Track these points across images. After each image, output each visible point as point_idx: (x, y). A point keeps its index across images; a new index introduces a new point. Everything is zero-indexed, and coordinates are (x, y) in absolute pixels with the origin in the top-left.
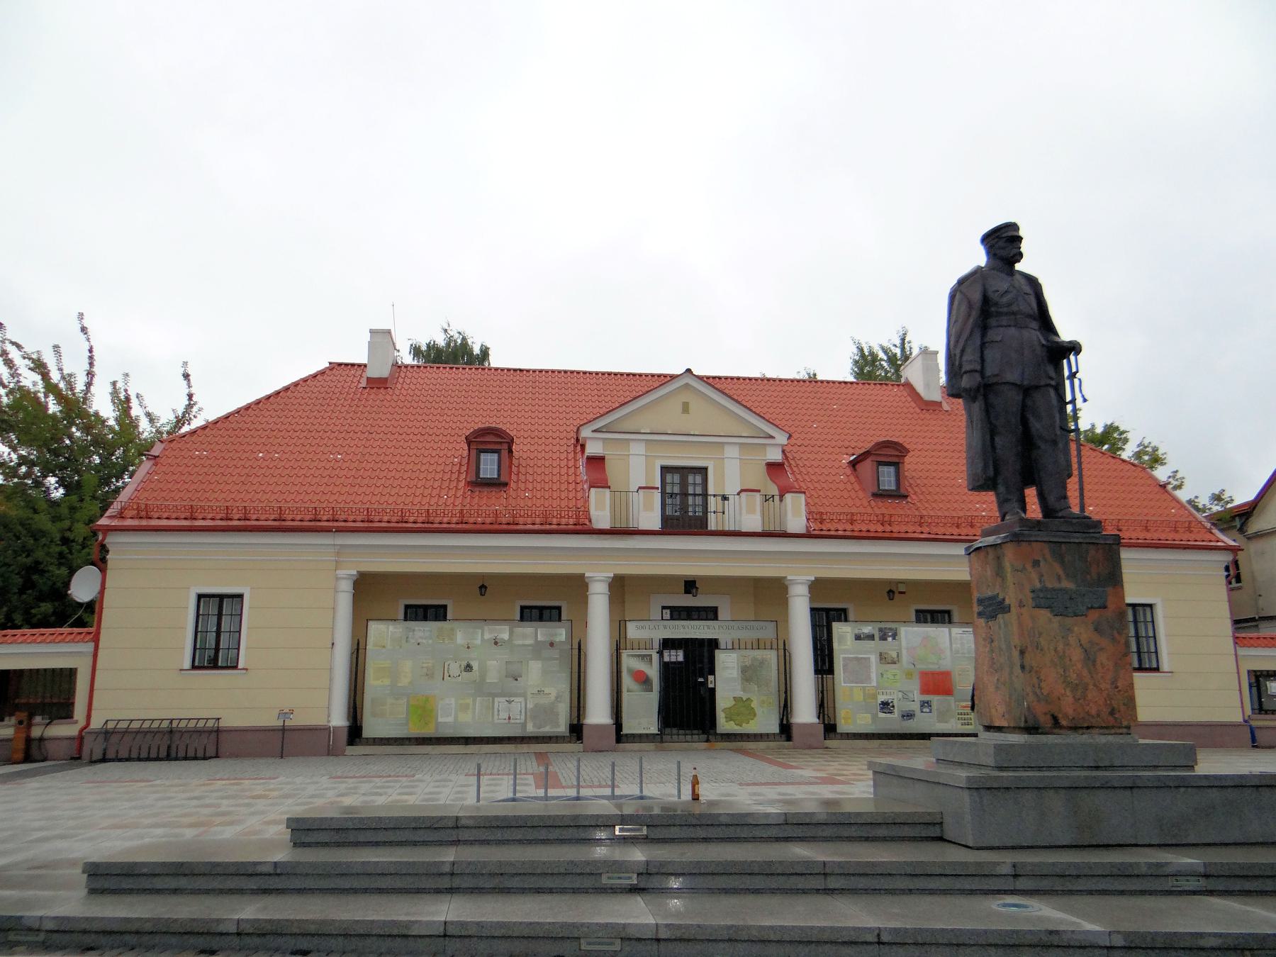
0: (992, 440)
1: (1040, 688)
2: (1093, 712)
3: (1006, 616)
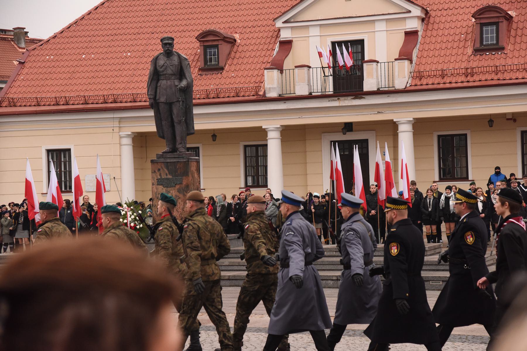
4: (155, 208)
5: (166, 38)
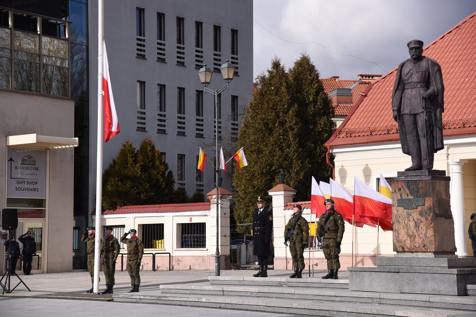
1: (398, 237)
2: (417, 246)
4: (395, 233)
5: (412, 42)
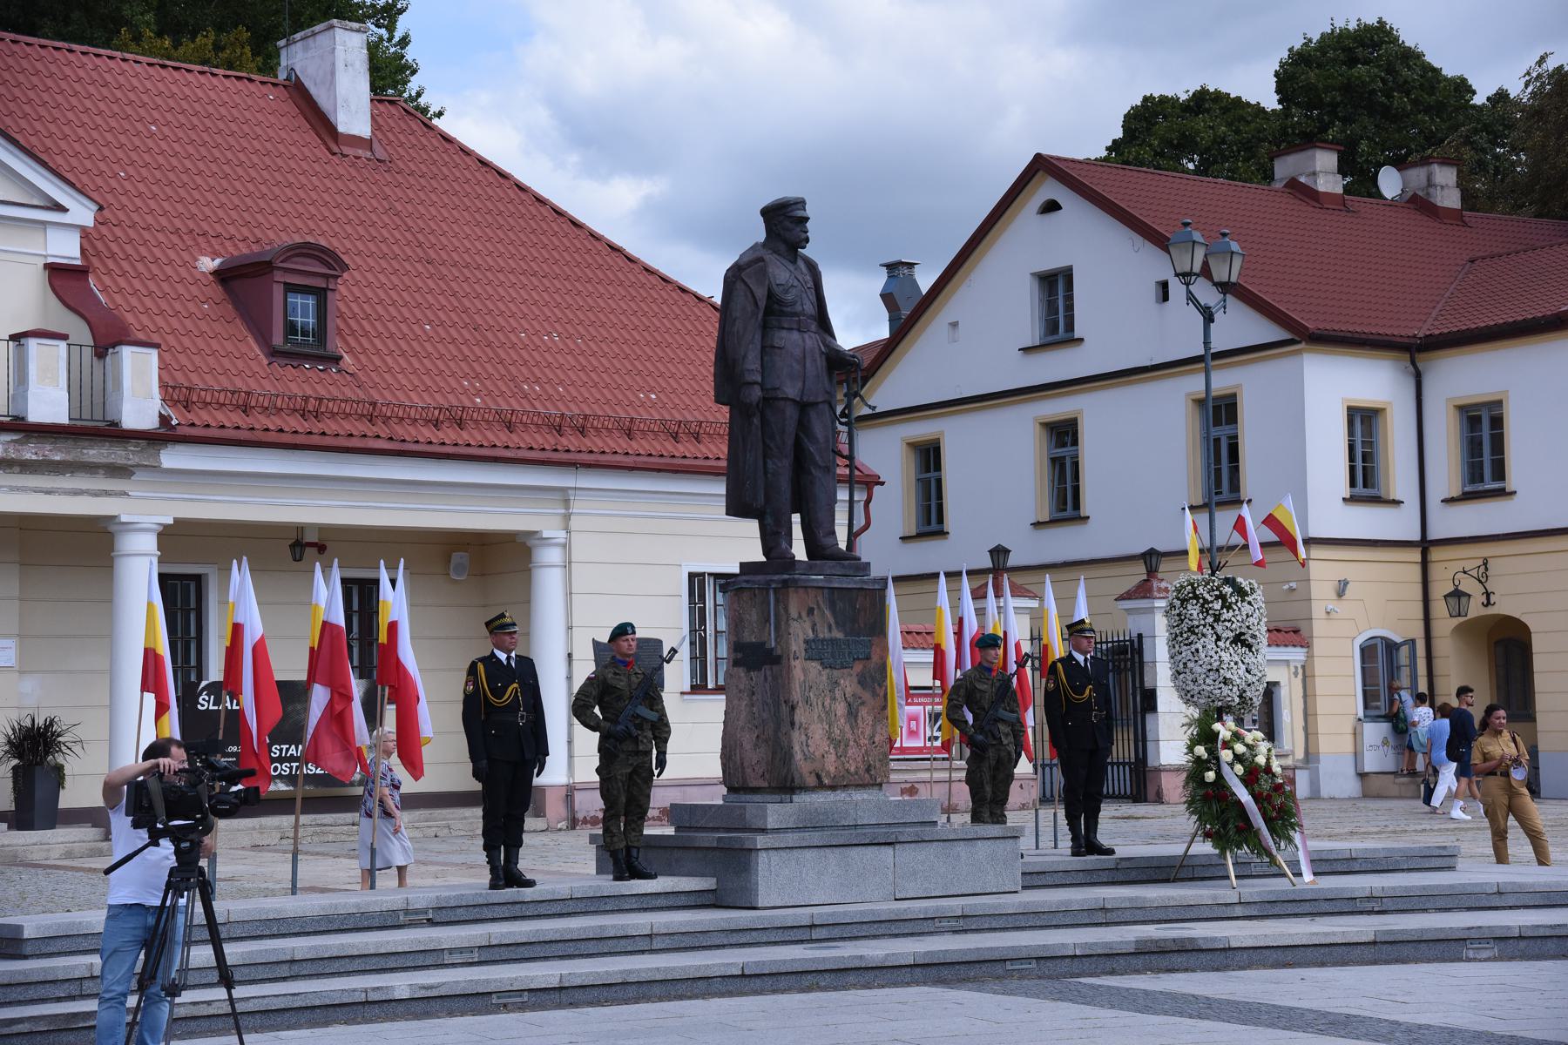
0: (765, 463)
1: (808, 746)
2: (852, 769)
3: (775, 668)
